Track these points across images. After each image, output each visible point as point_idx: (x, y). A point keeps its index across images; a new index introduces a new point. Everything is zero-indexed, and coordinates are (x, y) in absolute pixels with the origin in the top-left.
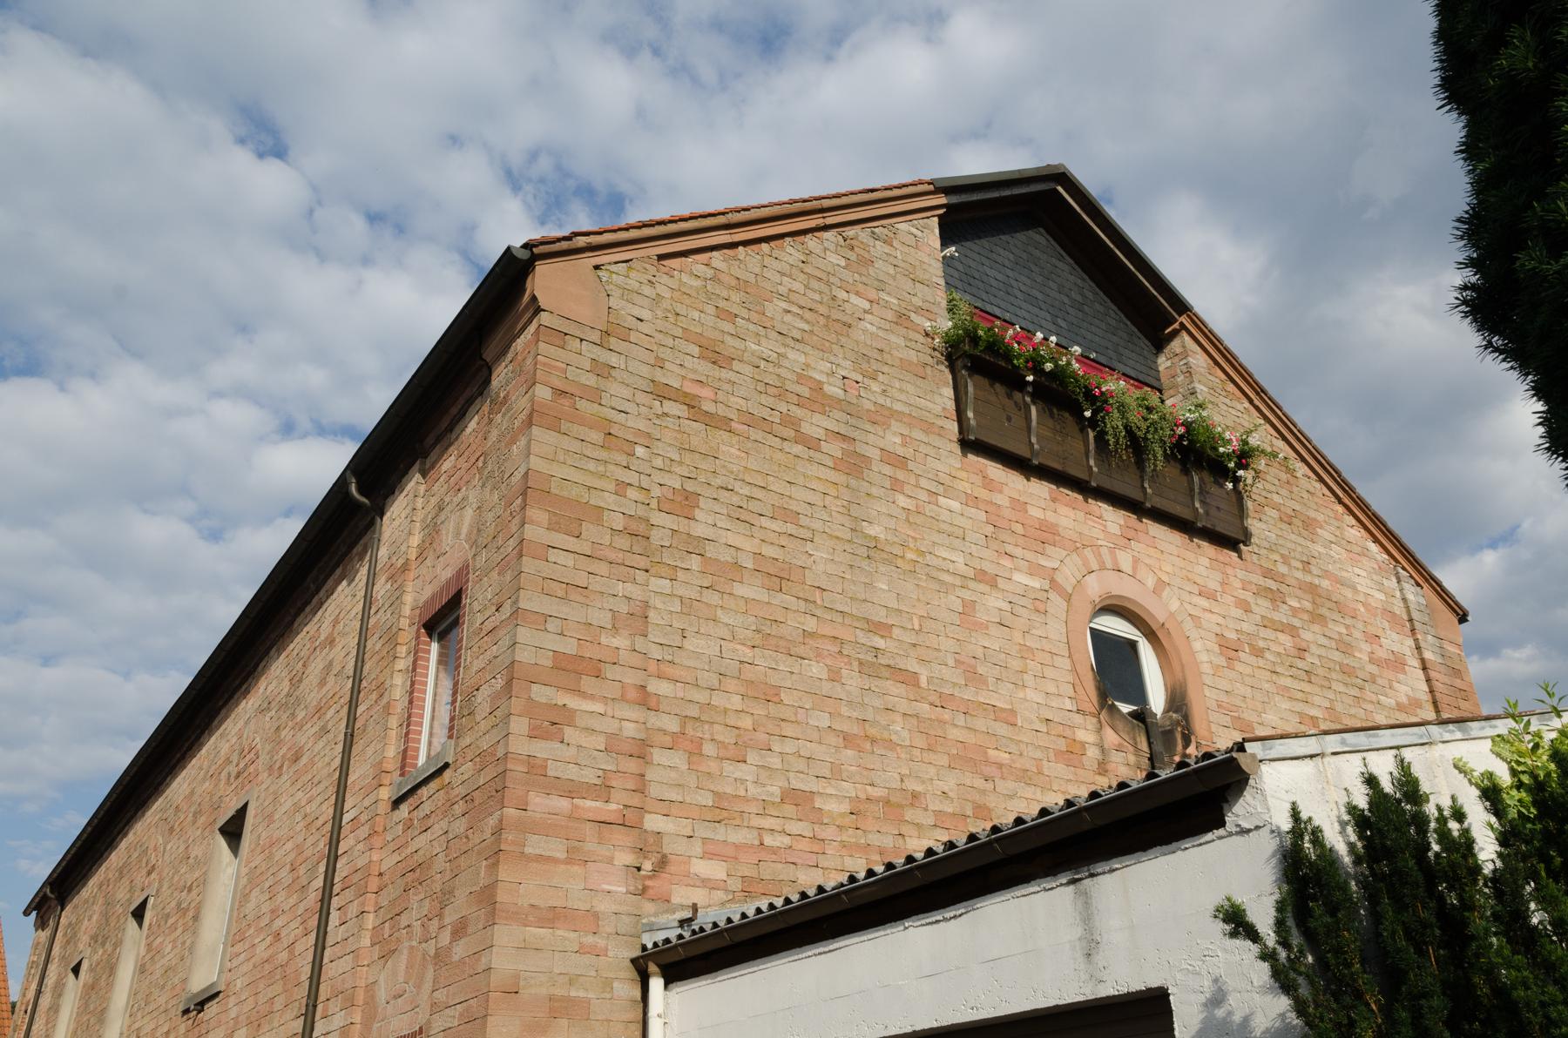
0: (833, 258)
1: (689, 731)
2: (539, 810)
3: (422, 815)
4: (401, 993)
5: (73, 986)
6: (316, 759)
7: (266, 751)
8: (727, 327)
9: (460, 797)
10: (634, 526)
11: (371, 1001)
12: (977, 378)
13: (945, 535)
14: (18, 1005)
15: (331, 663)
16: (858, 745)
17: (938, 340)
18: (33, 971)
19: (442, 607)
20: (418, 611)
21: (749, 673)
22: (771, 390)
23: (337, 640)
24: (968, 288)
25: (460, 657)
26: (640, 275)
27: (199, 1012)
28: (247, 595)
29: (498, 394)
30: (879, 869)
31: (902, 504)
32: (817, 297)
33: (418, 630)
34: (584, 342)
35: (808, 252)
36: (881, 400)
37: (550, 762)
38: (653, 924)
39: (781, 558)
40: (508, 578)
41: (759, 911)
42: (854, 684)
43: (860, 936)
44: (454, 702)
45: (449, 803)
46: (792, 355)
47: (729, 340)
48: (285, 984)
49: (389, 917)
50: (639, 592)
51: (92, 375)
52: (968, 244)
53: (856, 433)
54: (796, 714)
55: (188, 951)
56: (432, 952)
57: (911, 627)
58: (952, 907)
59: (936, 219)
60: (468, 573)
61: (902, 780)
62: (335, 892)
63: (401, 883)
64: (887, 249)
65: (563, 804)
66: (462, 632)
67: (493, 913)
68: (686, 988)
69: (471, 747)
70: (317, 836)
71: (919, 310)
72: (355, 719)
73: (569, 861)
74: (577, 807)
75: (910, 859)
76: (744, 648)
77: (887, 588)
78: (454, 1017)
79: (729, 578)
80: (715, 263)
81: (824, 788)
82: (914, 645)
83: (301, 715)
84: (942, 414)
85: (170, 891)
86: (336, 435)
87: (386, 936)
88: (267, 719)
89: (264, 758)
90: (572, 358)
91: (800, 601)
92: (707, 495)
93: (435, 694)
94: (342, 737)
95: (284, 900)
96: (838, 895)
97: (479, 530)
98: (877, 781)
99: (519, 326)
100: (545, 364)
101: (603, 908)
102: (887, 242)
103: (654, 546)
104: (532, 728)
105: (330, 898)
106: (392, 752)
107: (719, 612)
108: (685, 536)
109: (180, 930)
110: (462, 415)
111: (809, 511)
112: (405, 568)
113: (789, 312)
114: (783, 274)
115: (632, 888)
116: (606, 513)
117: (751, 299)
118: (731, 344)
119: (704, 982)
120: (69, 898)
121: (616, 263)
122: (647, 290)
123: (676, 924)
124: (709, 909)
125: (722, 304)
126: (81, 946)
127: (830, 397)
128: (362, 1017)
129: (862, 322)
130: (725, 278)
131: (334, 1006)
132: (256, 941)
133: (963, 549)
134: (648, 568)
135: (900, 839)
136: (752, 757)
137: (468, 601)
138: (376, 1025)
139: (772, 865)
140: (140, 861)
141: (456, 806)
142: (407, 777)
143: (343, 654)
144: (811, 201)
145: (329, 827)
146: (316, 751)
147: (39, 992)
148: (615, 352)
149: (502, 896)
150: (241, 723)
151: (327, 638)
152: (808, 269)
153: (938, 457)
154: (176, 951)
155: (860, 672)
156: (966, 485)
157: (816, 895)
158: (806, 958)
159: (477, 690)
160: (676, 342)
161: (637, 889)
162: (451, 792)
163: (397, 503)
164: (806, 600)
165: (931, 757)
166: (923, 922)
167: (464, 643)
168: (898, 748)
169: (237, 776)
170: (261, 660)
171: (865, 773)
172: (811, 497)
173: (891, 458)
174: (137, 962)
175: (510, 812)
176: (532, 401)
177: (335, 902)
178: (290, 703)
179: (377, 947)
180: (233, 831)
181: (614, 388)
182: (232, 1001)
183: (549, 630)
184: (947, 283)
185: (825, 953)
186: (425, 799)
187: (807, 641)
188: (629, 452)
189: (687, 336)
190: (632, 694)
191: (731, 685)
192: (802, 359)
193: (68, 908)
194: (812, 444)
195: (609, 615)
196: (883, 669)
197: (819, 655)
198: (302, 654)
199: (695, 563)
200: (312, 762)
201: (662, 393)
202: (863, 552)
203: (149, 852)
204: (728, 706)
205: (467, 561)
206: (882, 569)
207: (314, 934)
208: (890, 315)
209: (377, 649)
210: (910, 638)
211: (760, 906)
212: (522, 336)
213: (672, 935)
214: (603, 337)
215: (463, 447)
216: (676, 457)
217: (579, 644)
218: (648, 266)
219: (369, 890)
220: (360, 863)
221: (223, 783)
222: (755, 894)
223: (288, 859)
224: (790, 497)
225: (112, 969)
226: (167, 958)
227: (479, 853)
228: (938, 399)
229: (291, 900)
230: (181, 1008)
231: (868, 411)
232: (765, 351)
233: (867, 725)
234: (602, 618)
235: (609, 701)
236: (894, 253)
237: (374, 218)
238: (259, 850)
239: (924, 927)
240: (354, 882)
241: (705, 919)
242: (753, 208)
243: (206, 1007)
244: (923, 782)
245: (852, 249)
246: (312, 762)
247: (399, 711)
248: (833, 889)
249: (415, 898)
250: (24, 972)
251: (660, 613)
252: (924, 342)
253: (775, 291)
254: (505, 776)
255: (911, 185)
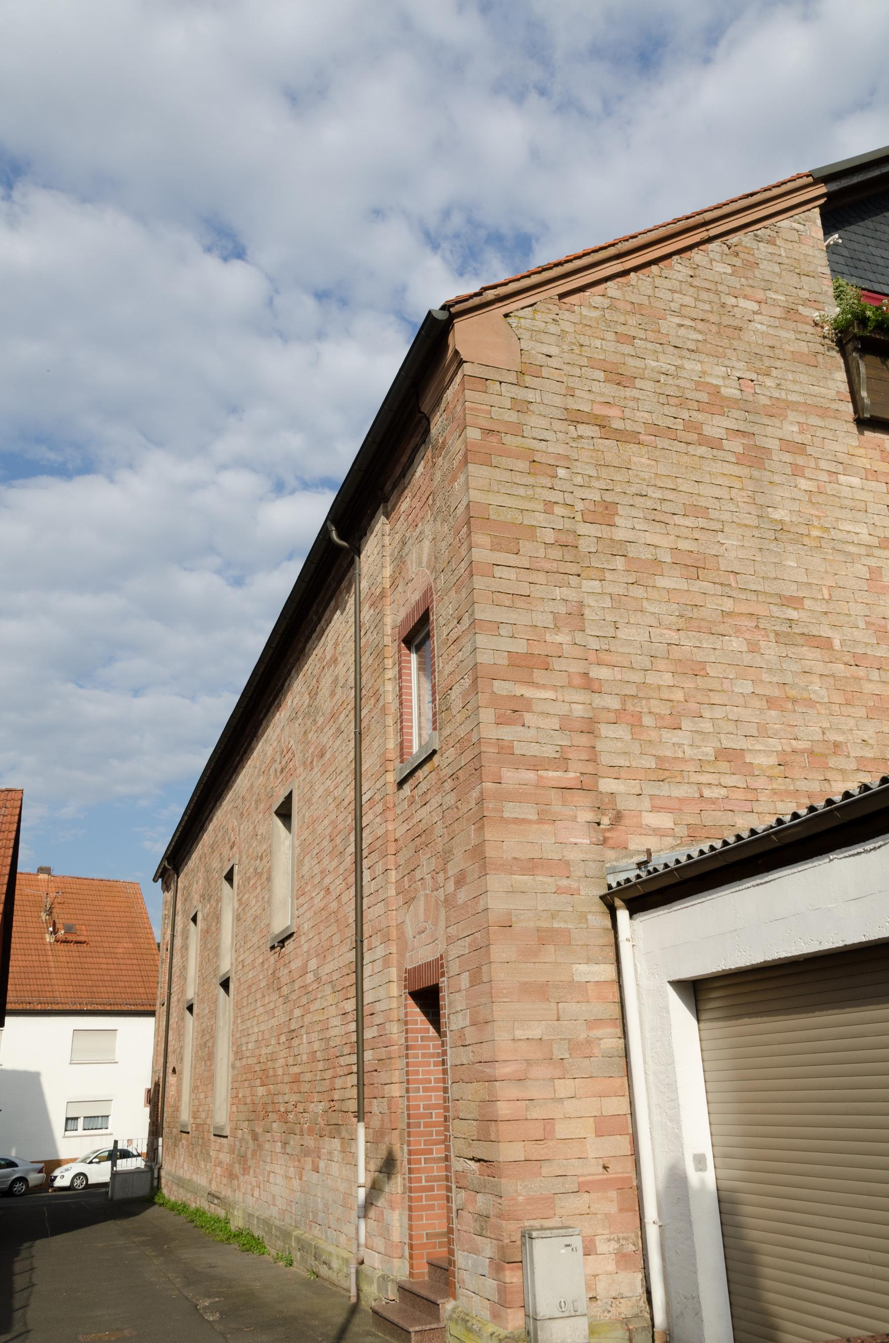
0: (720, 267)
1: (629, 707)
2: (511, 782)
3: (421, 792)
4: (423, 929)
5: (195, 932)
6: (337, 754)
7: (299, 751)
8: (627, 349)
9: (448, 776)
10: (563, 539)
11: (402, 936)
12: (870, 358)
13: (847, 510)
14: (161, 945)
15: (337, 677)
16: (782, 707)
17: (827, 328)
18: (166, 921)
19: (415, 624)
20: (397, 630)
21: (676, 653)
22: (673, 401)
23: (339, 659)
24: (854, 272)
25: (434, 663)
26: (544, 315)
27: (282, 948)
28: (269, 626)
29: (437, 440)
30: (803, 812)
31: (803, 487)
32: (707, 307)
33: (399, 645)
34: (503, 384)
35: (695, 266)
36: (776, 394)
37: (515, 743)
38: (615, 867)
39: (695, 549)
40: (464, 595)
41: (702, 852)
42: (773, 653)
43: (790, 869)
44: (434, 701)
45: (440, 782)
46: (688, 365)
47: (631, 361)
48: (338, 926)
49: (407, 872)
50: (574, 594)
51: (131, 466)
52: (852, 228)
53: (755, 428)
54: (722, 685)
55: (267, 904)
56: (442, 898)
57: (821, 597)
58: (871, 841)
59: (817, 210)
60: (432, 594)
61: (824, 733)
62: (364, 856)
63: (412, 846)
64: (771, 249)
65: (531, 776)
66: (433, 644)
67: (484, 866)
68: (648, 917)
69: (452, 736)
70: (345, 814)
71: (806, 302)
72: (361, 720)
73: (540, 821)
74: (541, 777)
75: (829, 802)
76: (669, 632)
77: (795, 565)
78: (465, 946)
79: (651, 573)
80: (610, 293)
81: (753, 745)
82: (826, 613)
83: (320, 720)
84: (837, 398)
85: (248, 861)
86: (317, 488)
87: (406, 887)
88: (297, 725)
89: (298, 756)
90: (495, 400)
91: (716, 585)
92: (624, 503)
93: (419, 696)
94: (353, 735)
95: (329, 863)
96: (768, 835)
97: (436, 558)
98: (800, 735)
99: (447, 379)
100: (472, 409)
101: (572, 857)
102: (771, 242)
103: (583, 553)
104: (498, 717)
105: (362, 860)
106: (392, 744)
107: (645, 604)
108: (608, 541)
109: (259, 889)
110: (411, 462)
111: (717, 504)
112: (382, 595)
113: (683, 325)
114: (673, 291)
115: (594, 840)
116: (538, 530)
117: (647, 320)
118: (633, 365)
119: (662, 912)
120: (182, 867)
121: (522, 308)
122: (552, 328)
123: (635, 866)
124: (661, 853)
125: (620, 329)
126: (195, 903)
127: (727, 398)
128: (397, 948)
129: (752, 323)
130: (620, 305)
131: (376, 941)
132: (314, 895)
133: (867, 521)
134: (579, 573)
135: (826, 784)
136: (686, 724)
137: (435, 617)
138: (408, 955)
139: (713, 813)
140: (224, 839)
141: (446, 784)
142: (406, 763)
143: (345, 668)
144: (694, 216)
145: (352, 806)
146: (336, 748)
147: (173, 936)
148: (530, 388)
149: (490, 852)
150: (278, 730)
151: (331, 658)
152: (696, 282)
153: (835, 439)
154: (259, 904)
155: (776, 642)
156: (865, 461)
157: (749, 837)
158: (746, 889)
159: (451, 689)
160: (583, 370)
161: (599, 839)
162: (440, 772)
163: (369, 542)
164: (721, 584)
165: (850, 710)
166: (846, 854)
167: (436, 652)
168: (817, 705)
169: (282, 772)
170: (285, 680)
171: (789, 729)
172: (718, 492)
173: (789, 446)
174: (233, 912)
175: (488, 785)
176: (465, 442)
177: (366, 863)
178: (311, 712)
179: (401, 896)
180: (285, 813)
181: (533, 420)
182: (303, 939)
183: (502, 634)
184: (832, 271)
185: (761, 884)
186: (421, 780)
187: (726, 620)
188: (552, 474)
189: (593, 364)
190: (577, 681)
191: (661, 664)
192: (698, 367)
193: (182, 875)
194: (715, 444)
195: (551, 616)
196: (798, 637)
197: (738, 631)
198: (315, 672)
199: (619, 563)
200: (334, 757)
201: (575, 418)
202: (771, 535)
203: (229, 832)
204: (661, 683)
205: (429, 584)
206: (790, 548)
207: (353, 888)
208: (778, 312)
209: (370, 663)
210: (821, 607)
211: (702, 848)
212: (451, 388)
213: (632, 875)
214: (519, 377)
215: (415, 489)
216: (593, 473)
217: (528, 644)
218: (550, 306)
219: (388, 853)
220: (380, 832)
221: (272, 777)
222: (699, 838)
223: (327, 832)
224: (699, 495)
225: (218, 918)
226: (254, 909)
227: (468, 820)
228: (831, 384)
229: (333, 863)
230: (269, 945)
231: (764, 405)
232: (664, 365)
233: (787, 688)
234: (543, 619)
235: (559, 689)
236: (777, 252)
237: (321, 296)
238: (305, 827)
239: (847, 859)
240: (377, 847)
241: (658, 862)
242: (640, 234)
243: (286, 944)
244: (844, 733)
245: (737, 255)
246: (334, 757)
247: (393, 711)
248: (764, 831)
249: (424, 857)
250: (161, 922)
251: (594, 610)
252: (814, 332)
253: (668, 308)
254: (480, 757)
255: (790, 181)
